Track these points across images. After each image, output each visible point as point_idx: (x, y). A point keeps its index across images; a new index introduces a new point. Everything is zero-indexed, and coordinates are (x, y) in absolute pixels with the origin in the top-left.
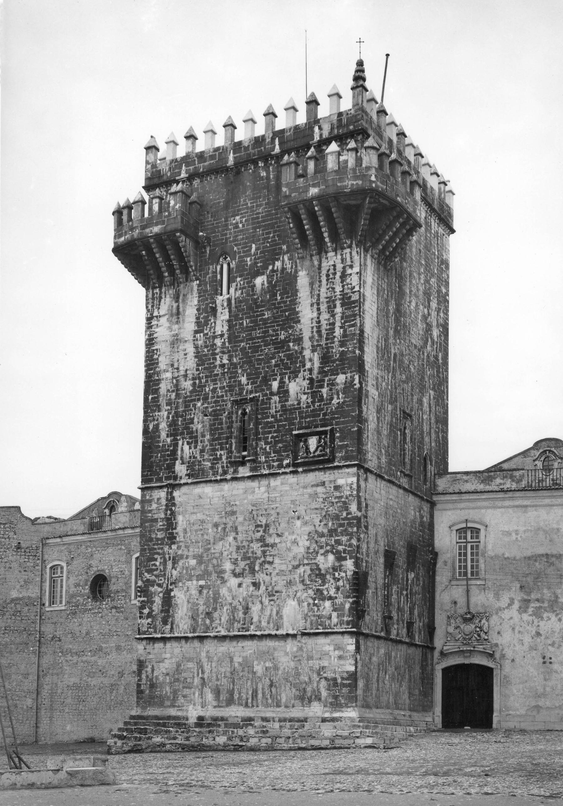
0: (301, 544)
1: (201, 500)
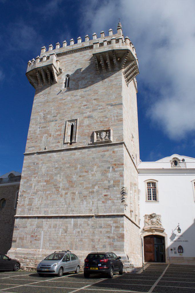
0: (97, 175)
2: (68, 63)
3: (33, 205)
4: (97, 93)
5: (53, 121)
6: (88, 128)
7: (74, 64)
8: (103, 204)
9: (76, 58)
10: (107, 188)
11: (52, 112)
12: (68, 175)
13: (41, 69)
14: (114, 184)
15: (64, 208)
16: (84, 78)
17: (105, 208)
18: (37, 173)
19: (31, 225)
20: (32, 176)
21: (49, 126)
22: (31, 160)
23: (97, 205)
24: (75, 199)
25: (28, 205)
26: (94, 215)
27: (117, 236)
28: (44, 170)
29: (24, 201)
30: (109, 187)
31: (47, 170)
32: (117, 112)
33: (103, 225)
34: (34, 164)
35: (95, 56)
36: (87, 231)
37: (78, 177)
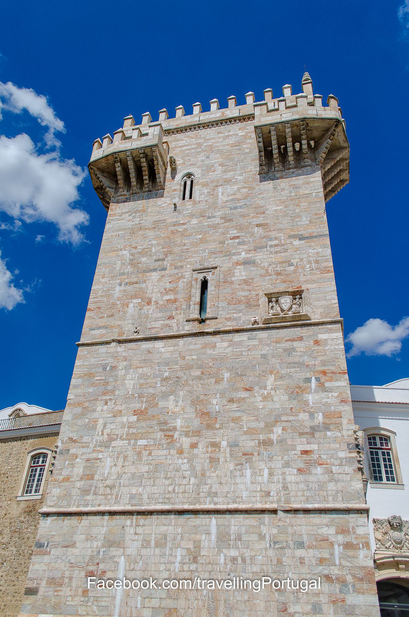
0: (276, 399)
1: (150, 355)
2: (188, 149)
3: (96, 477)
4: (264, 213)
5: (155, 270)
6: (246, 287)
7: (204, 151)
8: (301, 478)
9: (207, 140)
10: (307, 433)
11: (154, 251)
12: (198, 397)
13: (128, 153)
14: (327, 421)
15: (187, 487)
16: (231, 181)
17: (308, 486)
18: (113, 392)
19: (89, 538)
20: (97, 399)
21: (145, 282)
22: (97, 360)
23: (284, 479)
24: (219, 461)
25: (82, 479)
26: (274, 506)
27: (354, 576)
28: (130, 384)
29: (73, 466)
30: (314, 430)
31: (141, 385)
32: (318, 253)
33: (305, 538)
34: (105, 369)
35: (259, 131)
36: (260, 557)
37: (225, 402)
